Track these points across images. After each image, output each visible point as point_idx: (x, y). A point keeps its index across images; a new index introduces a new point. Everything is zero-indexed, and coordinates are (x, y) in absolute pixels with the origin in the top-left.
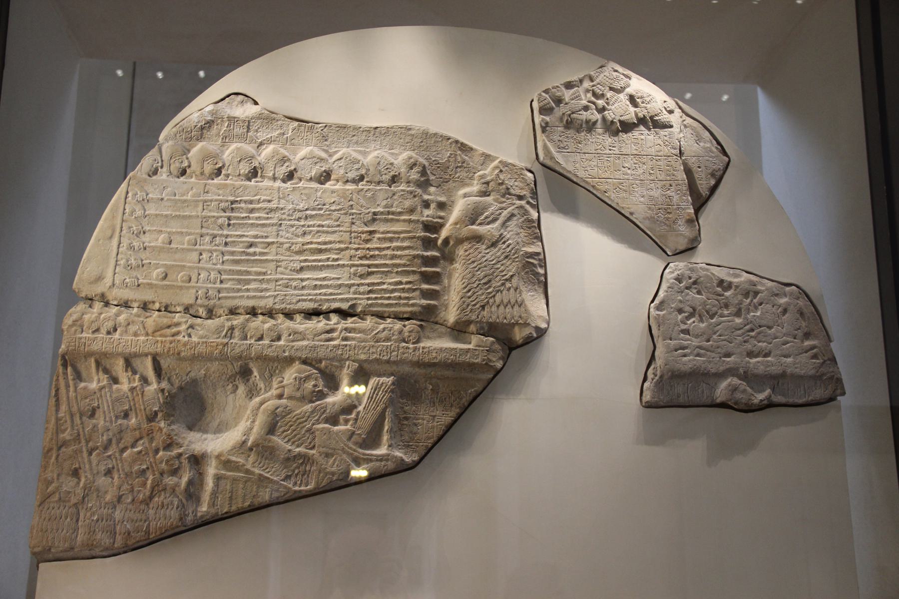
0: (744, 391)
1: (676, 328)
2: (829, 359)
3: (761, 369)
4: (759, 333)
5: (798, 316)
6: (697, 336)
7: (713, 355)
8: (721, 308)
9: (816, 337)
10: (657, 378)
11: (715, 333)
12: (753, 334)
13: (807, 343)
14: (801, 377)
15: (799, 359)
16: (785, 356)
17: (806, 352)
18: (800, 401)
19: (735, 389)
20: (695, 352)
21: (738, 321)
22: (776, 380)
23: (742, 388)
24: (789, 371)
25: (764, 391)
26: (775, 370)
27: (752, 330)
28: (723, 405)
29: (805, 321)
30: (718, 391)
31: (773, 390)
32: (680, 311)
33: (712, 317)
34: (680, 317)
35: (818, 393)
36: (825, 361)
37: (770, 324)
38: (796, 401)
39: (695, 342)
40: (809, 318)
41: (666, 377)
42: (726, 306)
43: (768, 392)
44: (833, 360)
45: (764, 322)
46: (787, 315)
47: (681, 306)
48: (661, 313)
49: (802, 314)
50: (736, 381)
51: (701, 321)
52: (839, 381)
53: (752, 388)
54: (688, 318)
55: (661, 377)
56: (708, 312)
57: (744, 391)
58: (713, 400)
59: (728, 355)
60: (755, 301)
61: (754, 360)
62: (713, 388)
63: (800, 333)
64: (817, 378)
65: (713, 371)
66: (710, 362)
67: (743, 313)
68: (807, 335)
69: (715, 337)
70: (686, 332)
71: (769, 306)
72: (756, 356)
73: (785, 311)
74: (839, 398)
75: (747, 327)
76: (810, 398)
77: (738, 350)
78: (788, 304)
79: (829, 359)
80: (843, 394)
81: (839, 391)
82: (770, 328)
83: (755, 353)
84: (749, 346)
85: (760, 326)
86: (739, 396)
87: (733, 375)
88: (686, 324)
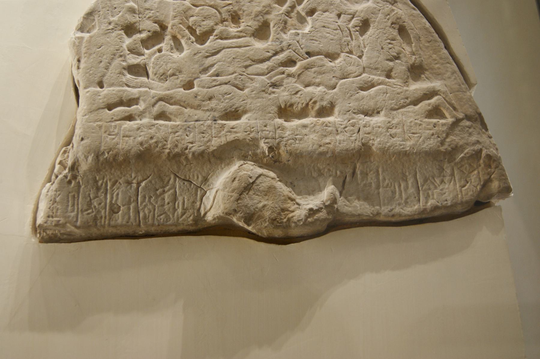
0: (271, 189)
1: (117, 61)
2: (468, 118)
3: (310, 142)
4: (307, 68)
5: (395, 33)
6: (164, 77)
7: (199, 114)
8: (223, 21)
9: (438, 75)
10: (67, 171)
11: (205, 70)
12: (293, 70)
13: (417, 87)
14: (406, 154)
15: (398, 117)
16: (366, 114)
17: (415, 103)
18: (411, 210)
19: (248, 187)
20: (156, 109)
21: (259, 45)
22: (351, 164)
23: (264, 183)
24: (376, 143)
25: (320, 190)
26: (344, 141)
27: (291, 62)
28: (223, 229)
29: (410, 43)
30: (210, 195)
31: (342, 187)
32: (130, 29)
33: (202, 38)
34: (128, 41)
35: (449, 191)
36: (457, 122)
37: (332, 48)
38: (397, 210)
39: (159, 88)
40: (418, 39)
41: (84, 167)
42: (235, 18)
43: (328, 191)
44: (477, 119)
45: (315, 46)
46: (371, 31)
47: (131, 18)
48: (86, 35)
49: (402, 30)
50: (251, 169)
51: (177, 46)
52: (492, 161)
53: (291, 185)
54: (147, 43)
55: (74, 167)
56: (192, 30)
57: (271, 189)
58: (199, 218)
59: (234, 114)
60: (299, 8)
61: (296, 122)
62: (199, 190)
63: (400, 67)
64: (442, 157)
65: (196, 148)
66: (187, 130)
67: (272, 30)
68: (416, 71)
69: (204, 77)
70: (138, 70)
71: (331, 16)
72: (303, 113)
73: (365, 25)
74: (497, 202)
75: (281, 57)
76: (431, 203)
77: (258, 103)
78: (374, 12)
79: (468, 118)
80: (506, 191)
81: (495, 185)
82: (332, 56)
83: (297, 108)
84: (282, 95)
85: (309, 54)
86: (255, 201)
87: (245, 158)
88: (140, 54)
